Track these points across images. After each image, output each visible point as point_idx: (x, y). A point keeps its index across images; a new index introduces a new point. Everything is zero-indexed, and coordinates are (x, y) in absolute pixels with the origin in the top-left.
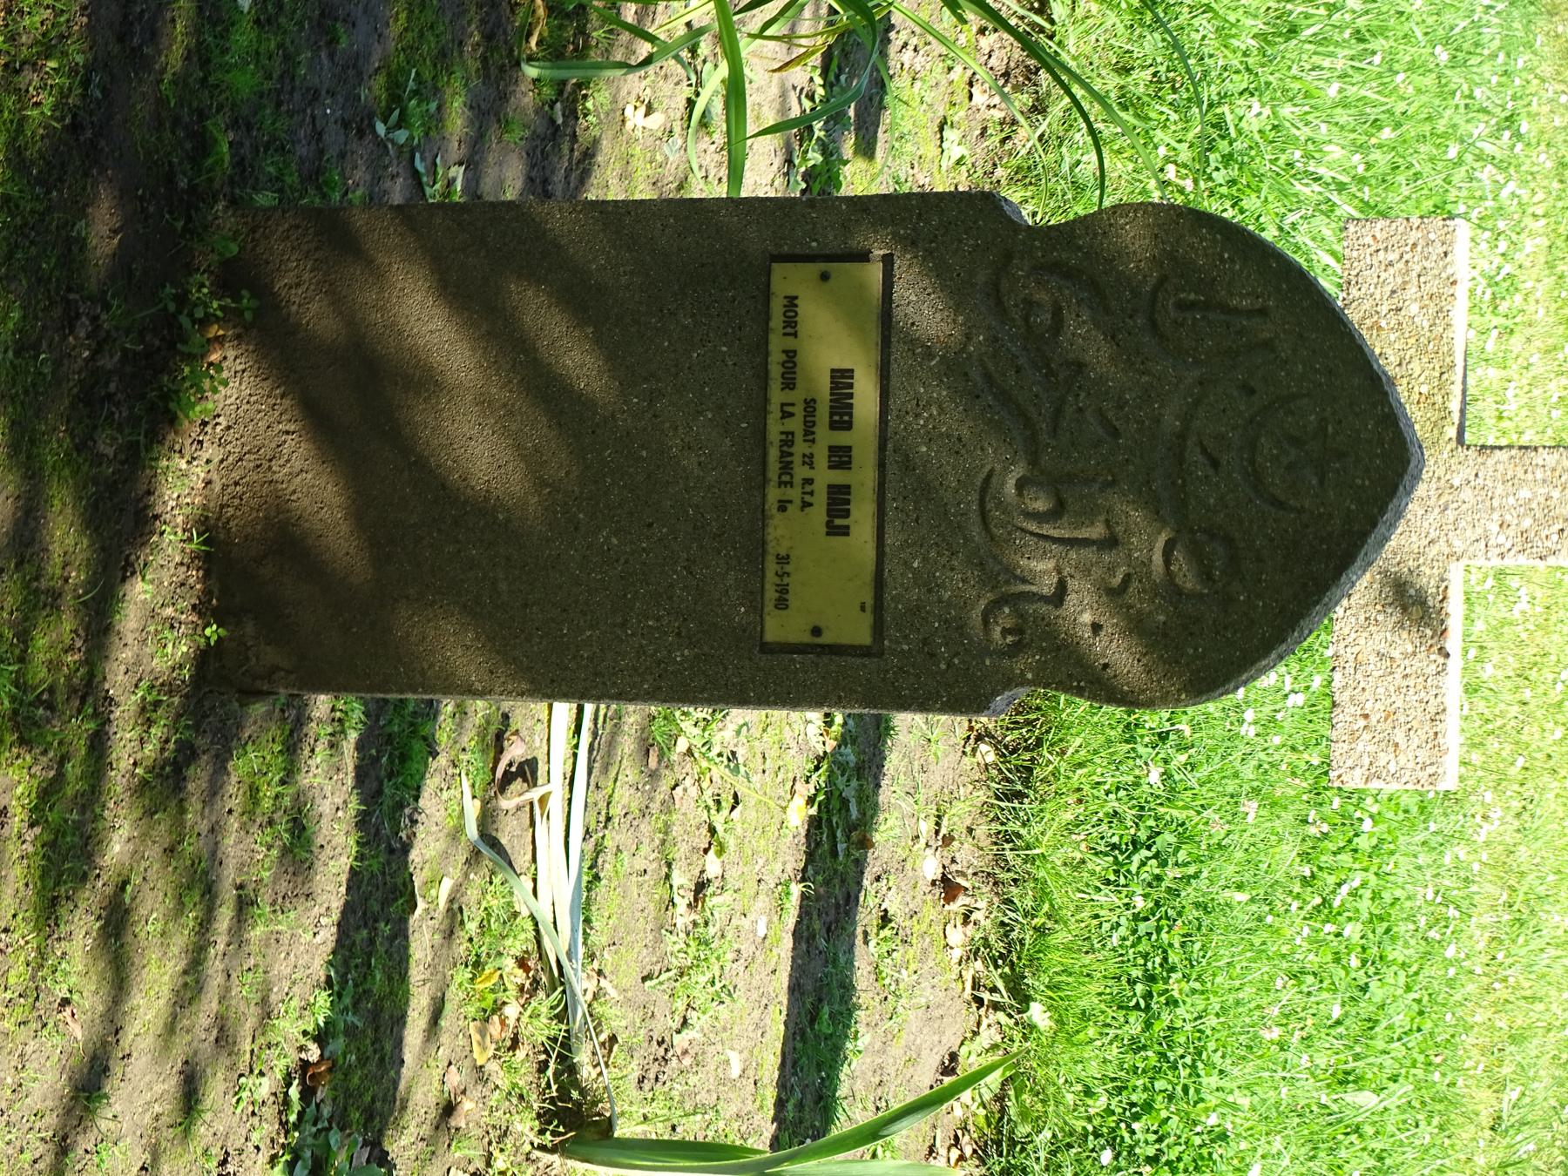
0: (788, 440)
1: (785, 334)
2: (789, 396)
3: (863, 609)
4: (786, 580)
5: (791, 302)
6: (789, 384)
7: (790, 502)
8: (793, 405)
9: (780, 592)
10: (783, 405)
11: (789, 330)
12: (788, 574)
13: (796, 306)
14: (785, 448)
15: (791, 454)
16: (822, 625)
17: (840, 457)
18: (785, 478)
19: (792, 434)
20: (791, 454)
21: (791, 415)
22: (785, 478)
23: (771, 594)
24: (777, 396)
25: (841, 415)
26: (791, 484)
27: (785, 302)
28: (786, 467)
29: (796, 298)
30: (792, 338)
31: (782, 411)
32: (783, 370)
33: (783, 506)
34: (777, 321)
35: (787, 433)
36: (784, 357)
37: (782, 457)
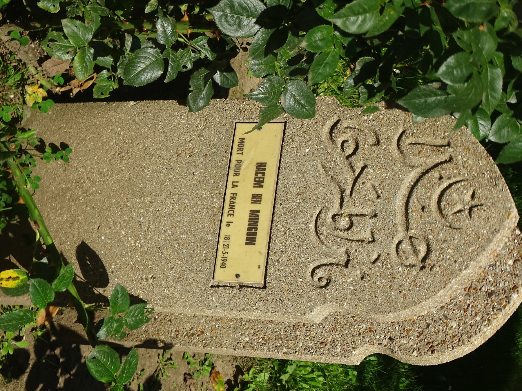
0: (234, 196)
1: (237, 154)
2: (236, 179)
4: (226, 255)
7: (232, 222)
8: (238, 182)
9: (223, 261)
10: (233, 182)
12: (228, 253)
13: (244, 142)
14: (232, 200)
15: (234, 203)
17: (257, 198)
18: (231, 212)
19: (236, 194)
20: (234, 203)
21: (237, 186)
22: (231, 212)
24: (231, 178)
26: (233, 215)
28: (232, 208)
29: (244, 139)
30: (241, 155)
31: (233, 185)
33: (228, 225)
34: (235, 147)
35: (234, 194)
36: (236, 163)
37: (230, 204)
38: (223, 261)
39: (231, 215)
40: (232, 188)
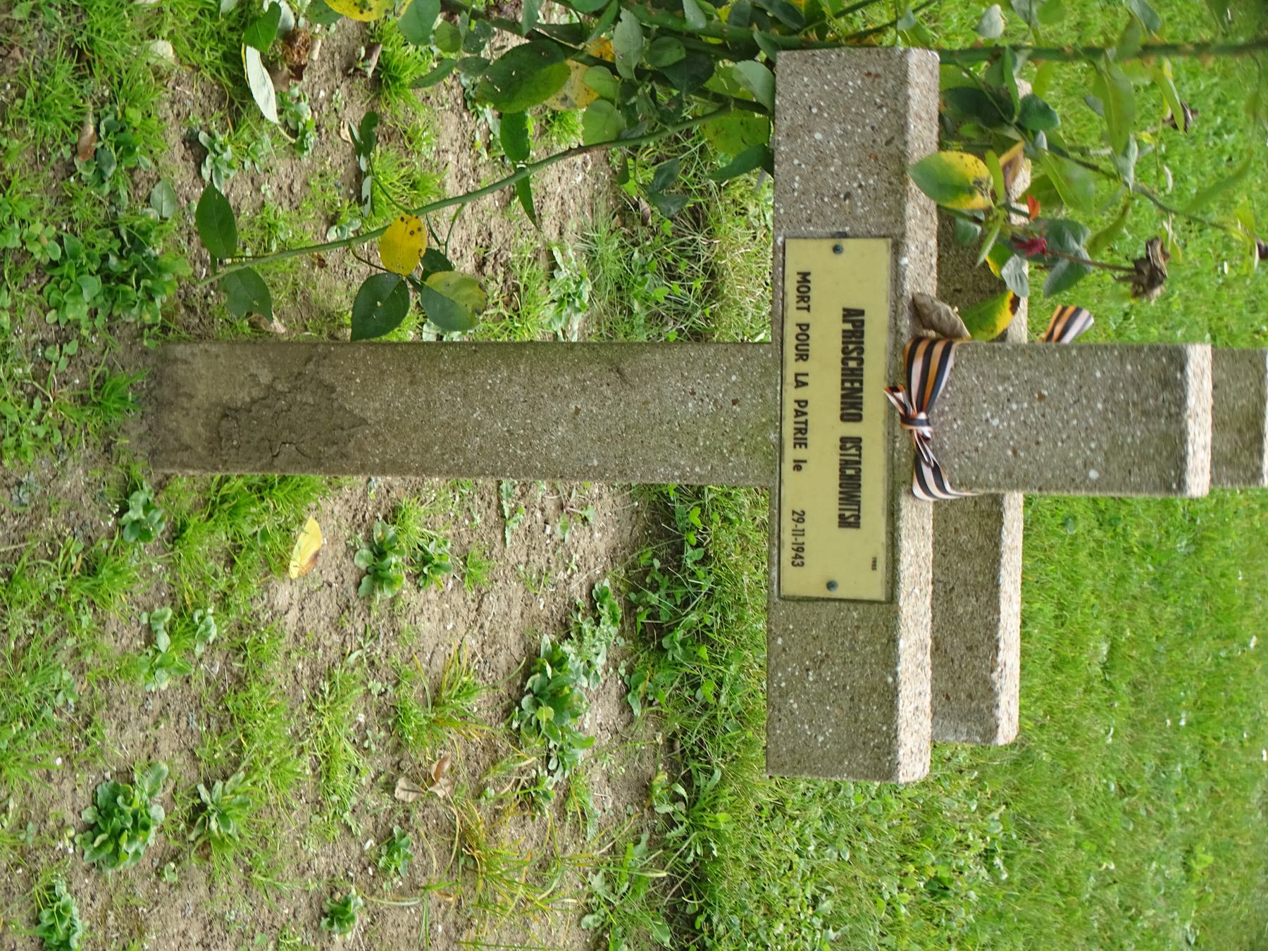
2: (802, 366)
3: (874, 567)
4: (800, 540)
5: (804, 277)
6: (803, 356)
9: (797, 550)
10: (797, 375)
11: (803, 304)
16: (837, 579)
21: (805, 384)
23: (787, 554)
24: (792, 367)
25: (852, 382)
27: (799, 278)
29: (809, 274)
32: (796, 342)
36: (798, 331)
38: (797, 550)
39: (800, 445)
40: (797, 386)
